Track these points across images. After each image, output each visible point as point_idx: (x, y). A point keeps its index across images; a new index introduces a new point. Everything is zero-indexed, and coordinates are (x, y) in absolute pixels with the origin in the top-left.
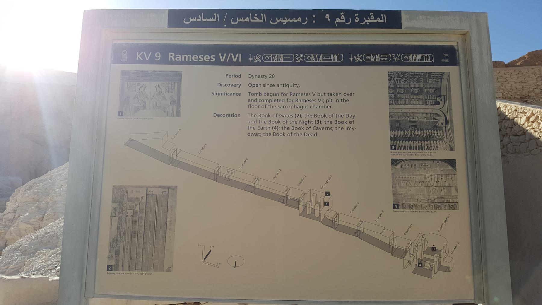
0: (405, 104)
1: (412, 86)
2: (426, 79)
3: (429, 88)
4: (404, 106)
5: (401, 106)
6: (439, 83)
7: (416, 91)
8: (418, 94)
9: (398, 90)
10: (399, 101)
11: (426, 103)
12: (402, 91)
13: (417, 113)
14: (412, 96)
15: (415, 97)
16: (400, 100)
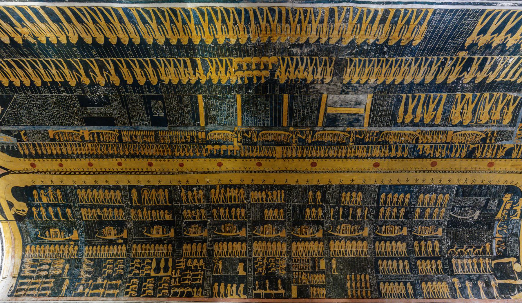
0: (139, 189)
1: (121, 250)
2: (70, 274)
3: (64, 243)
4: (143, 180)
5: (154, 180)
6: (28, 261)
7: (110, 233)
8: (101, 224)
9: (172, 234)
10: (163, 196)
11: (65, 195)
12: (156, 232)
13: (89, 156)
14: (120, 215)
15: (108, 214)
16: (162, 203)
